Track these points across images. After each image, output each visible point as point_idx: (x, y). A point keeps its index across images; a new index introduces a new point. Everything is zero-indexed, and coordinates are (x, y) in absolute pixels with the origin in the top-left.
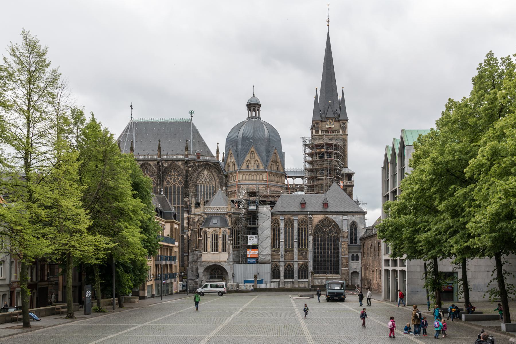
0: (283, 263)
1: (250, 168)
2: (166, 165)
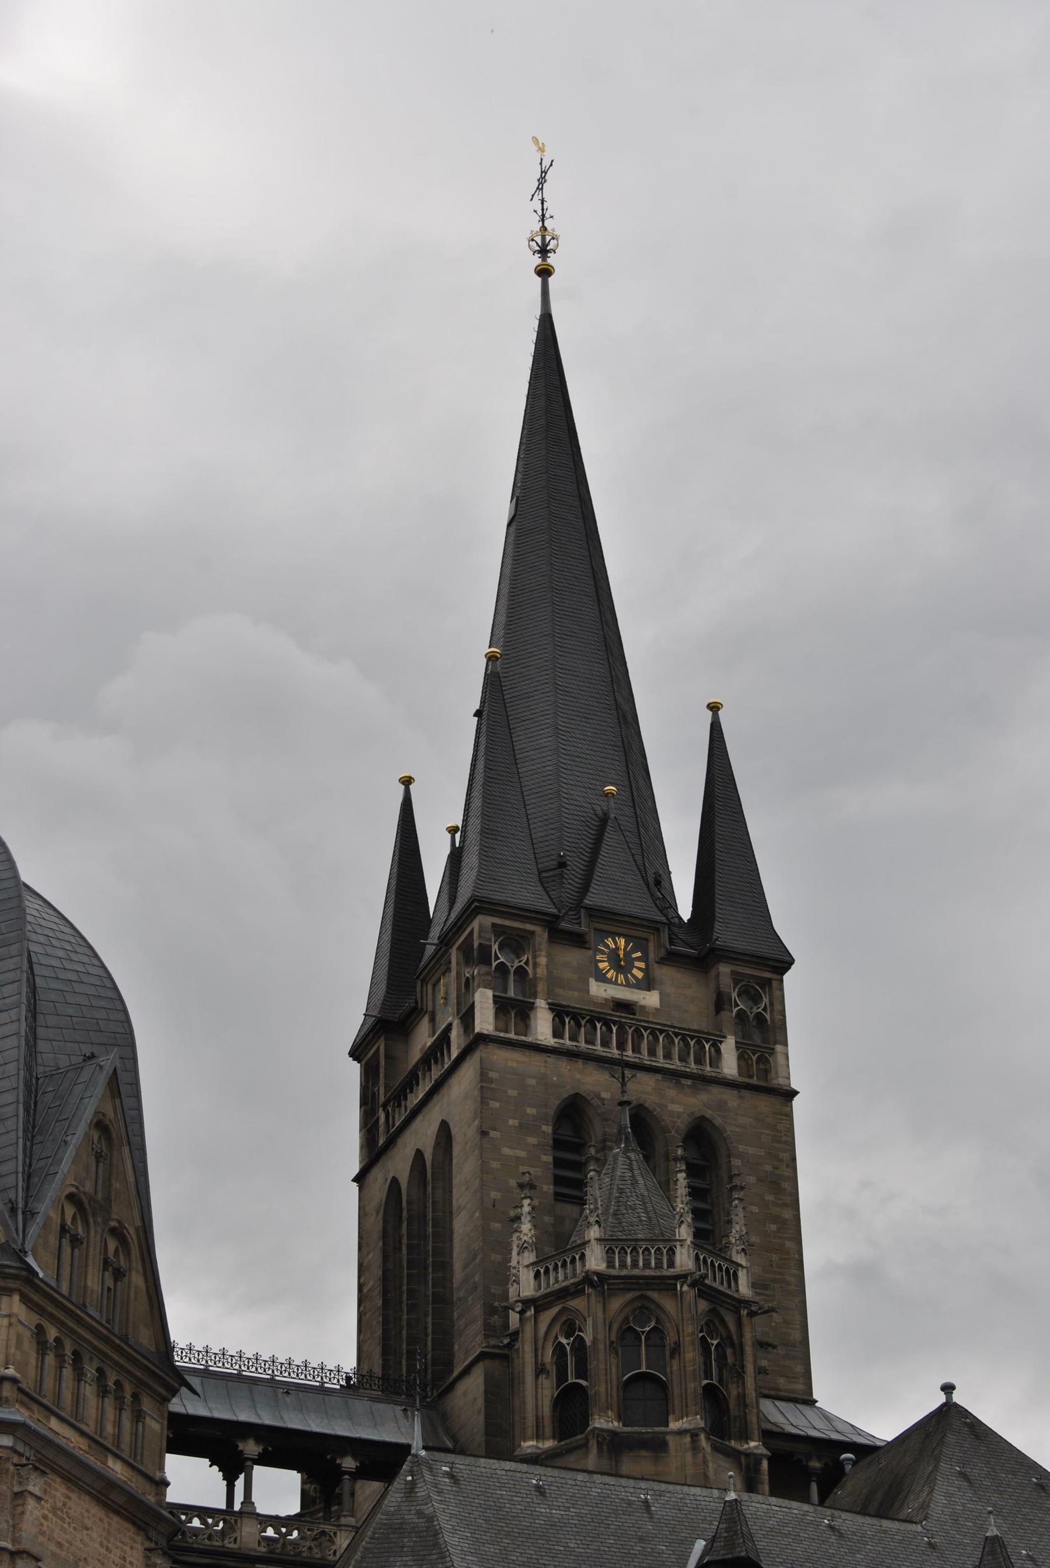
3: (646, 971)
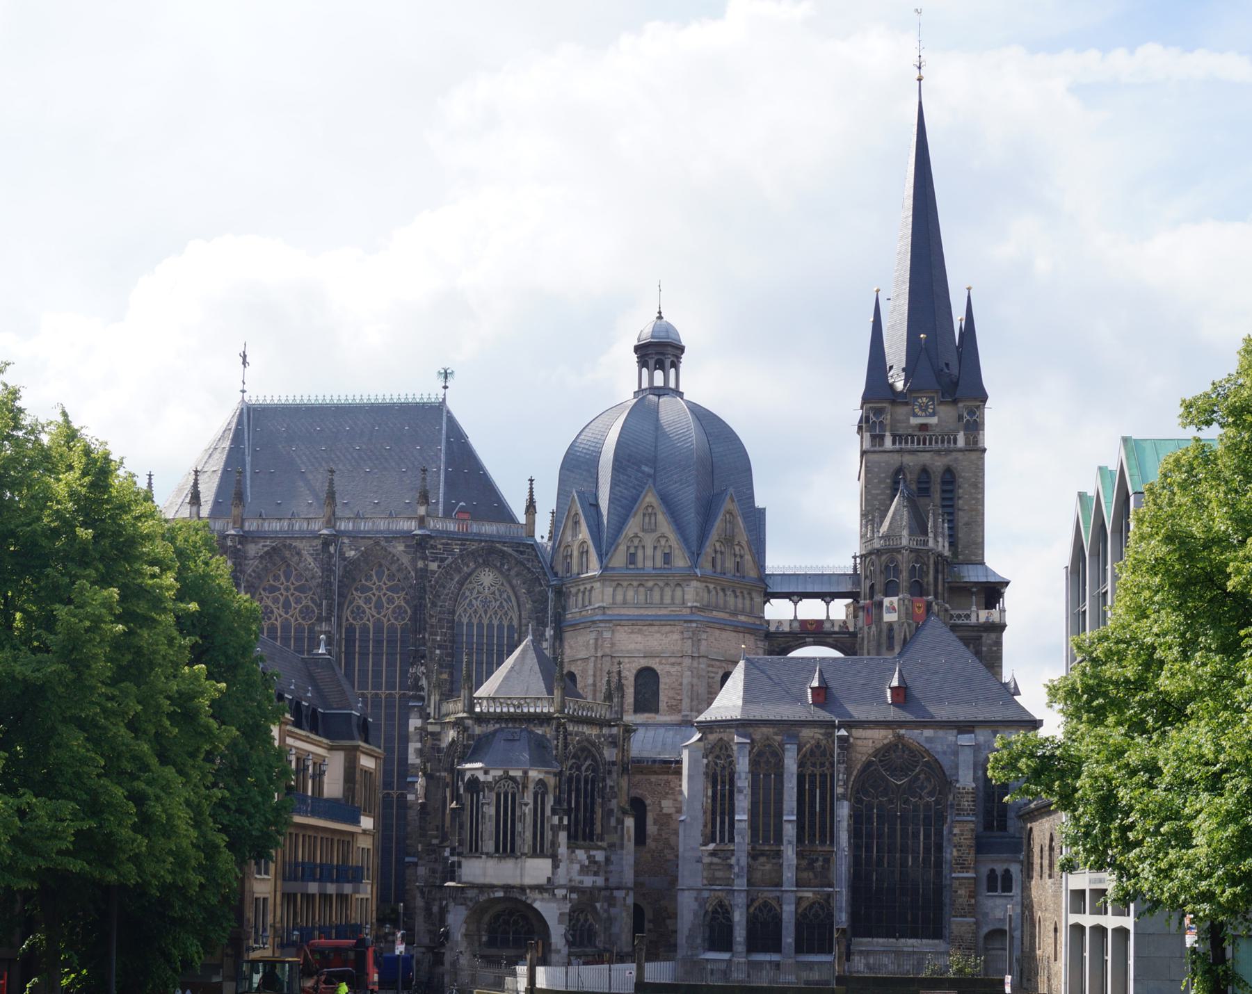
0: (743, 895)
1: (640, 565)
3: (933, 409)
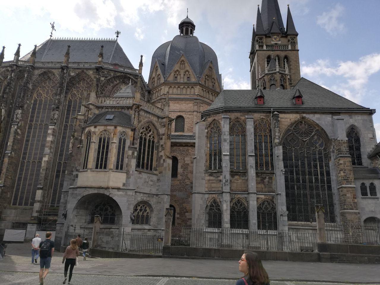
0: (228, 195)
2: (72, 74)
